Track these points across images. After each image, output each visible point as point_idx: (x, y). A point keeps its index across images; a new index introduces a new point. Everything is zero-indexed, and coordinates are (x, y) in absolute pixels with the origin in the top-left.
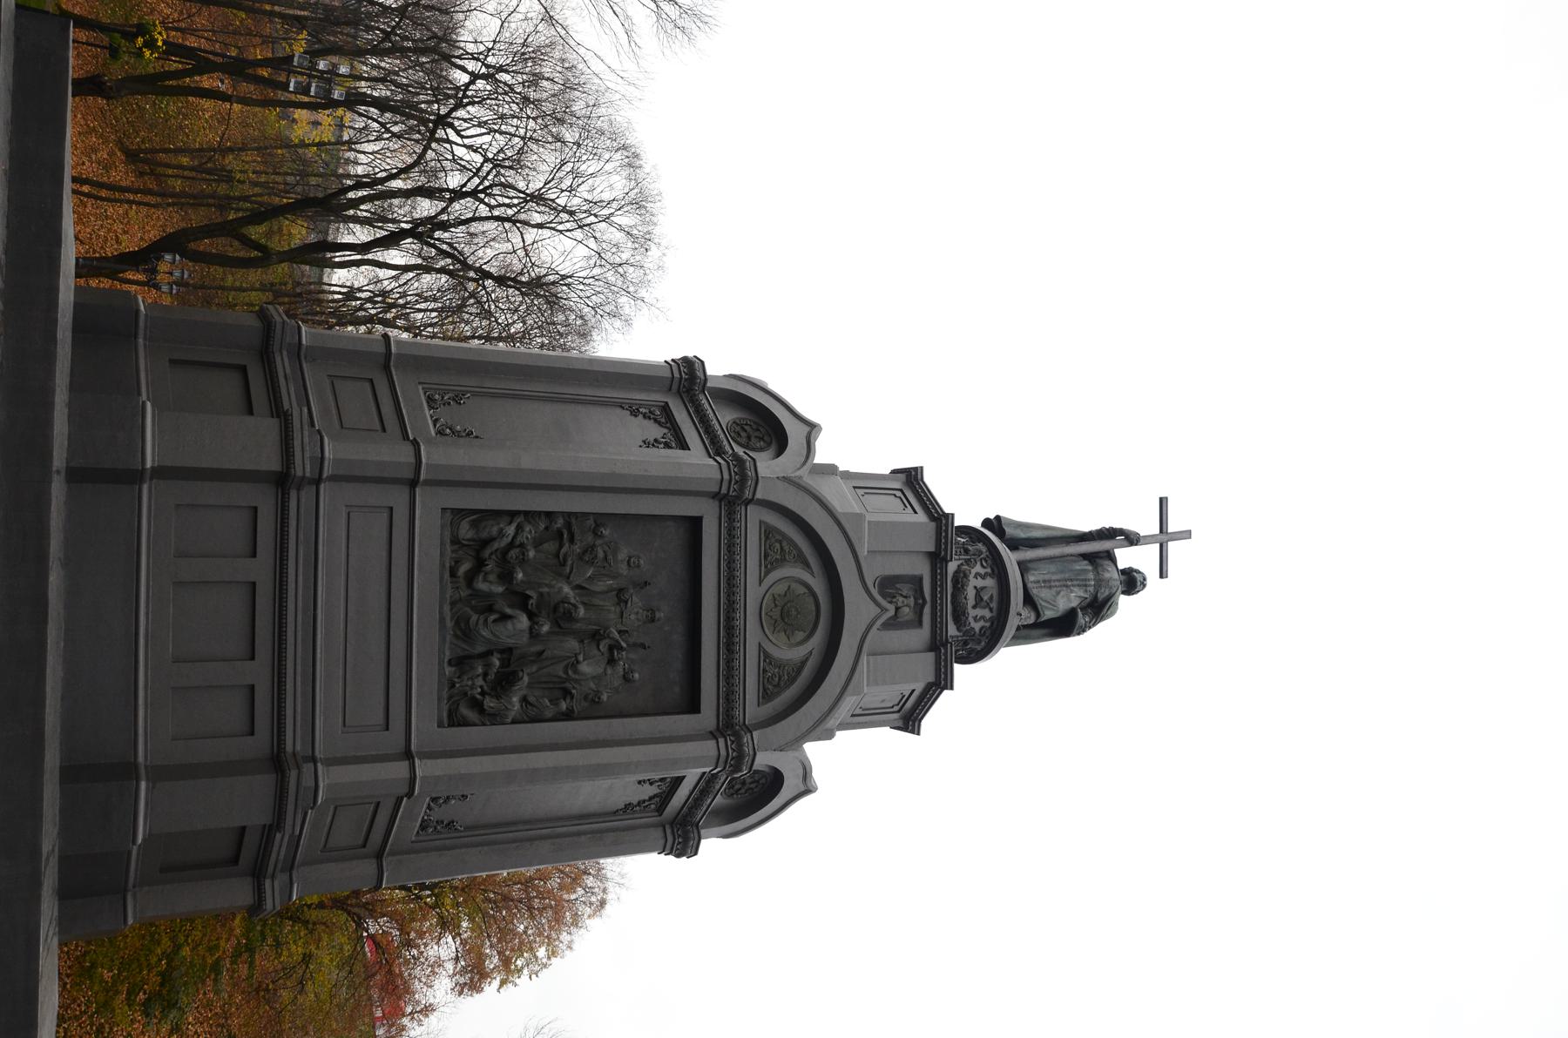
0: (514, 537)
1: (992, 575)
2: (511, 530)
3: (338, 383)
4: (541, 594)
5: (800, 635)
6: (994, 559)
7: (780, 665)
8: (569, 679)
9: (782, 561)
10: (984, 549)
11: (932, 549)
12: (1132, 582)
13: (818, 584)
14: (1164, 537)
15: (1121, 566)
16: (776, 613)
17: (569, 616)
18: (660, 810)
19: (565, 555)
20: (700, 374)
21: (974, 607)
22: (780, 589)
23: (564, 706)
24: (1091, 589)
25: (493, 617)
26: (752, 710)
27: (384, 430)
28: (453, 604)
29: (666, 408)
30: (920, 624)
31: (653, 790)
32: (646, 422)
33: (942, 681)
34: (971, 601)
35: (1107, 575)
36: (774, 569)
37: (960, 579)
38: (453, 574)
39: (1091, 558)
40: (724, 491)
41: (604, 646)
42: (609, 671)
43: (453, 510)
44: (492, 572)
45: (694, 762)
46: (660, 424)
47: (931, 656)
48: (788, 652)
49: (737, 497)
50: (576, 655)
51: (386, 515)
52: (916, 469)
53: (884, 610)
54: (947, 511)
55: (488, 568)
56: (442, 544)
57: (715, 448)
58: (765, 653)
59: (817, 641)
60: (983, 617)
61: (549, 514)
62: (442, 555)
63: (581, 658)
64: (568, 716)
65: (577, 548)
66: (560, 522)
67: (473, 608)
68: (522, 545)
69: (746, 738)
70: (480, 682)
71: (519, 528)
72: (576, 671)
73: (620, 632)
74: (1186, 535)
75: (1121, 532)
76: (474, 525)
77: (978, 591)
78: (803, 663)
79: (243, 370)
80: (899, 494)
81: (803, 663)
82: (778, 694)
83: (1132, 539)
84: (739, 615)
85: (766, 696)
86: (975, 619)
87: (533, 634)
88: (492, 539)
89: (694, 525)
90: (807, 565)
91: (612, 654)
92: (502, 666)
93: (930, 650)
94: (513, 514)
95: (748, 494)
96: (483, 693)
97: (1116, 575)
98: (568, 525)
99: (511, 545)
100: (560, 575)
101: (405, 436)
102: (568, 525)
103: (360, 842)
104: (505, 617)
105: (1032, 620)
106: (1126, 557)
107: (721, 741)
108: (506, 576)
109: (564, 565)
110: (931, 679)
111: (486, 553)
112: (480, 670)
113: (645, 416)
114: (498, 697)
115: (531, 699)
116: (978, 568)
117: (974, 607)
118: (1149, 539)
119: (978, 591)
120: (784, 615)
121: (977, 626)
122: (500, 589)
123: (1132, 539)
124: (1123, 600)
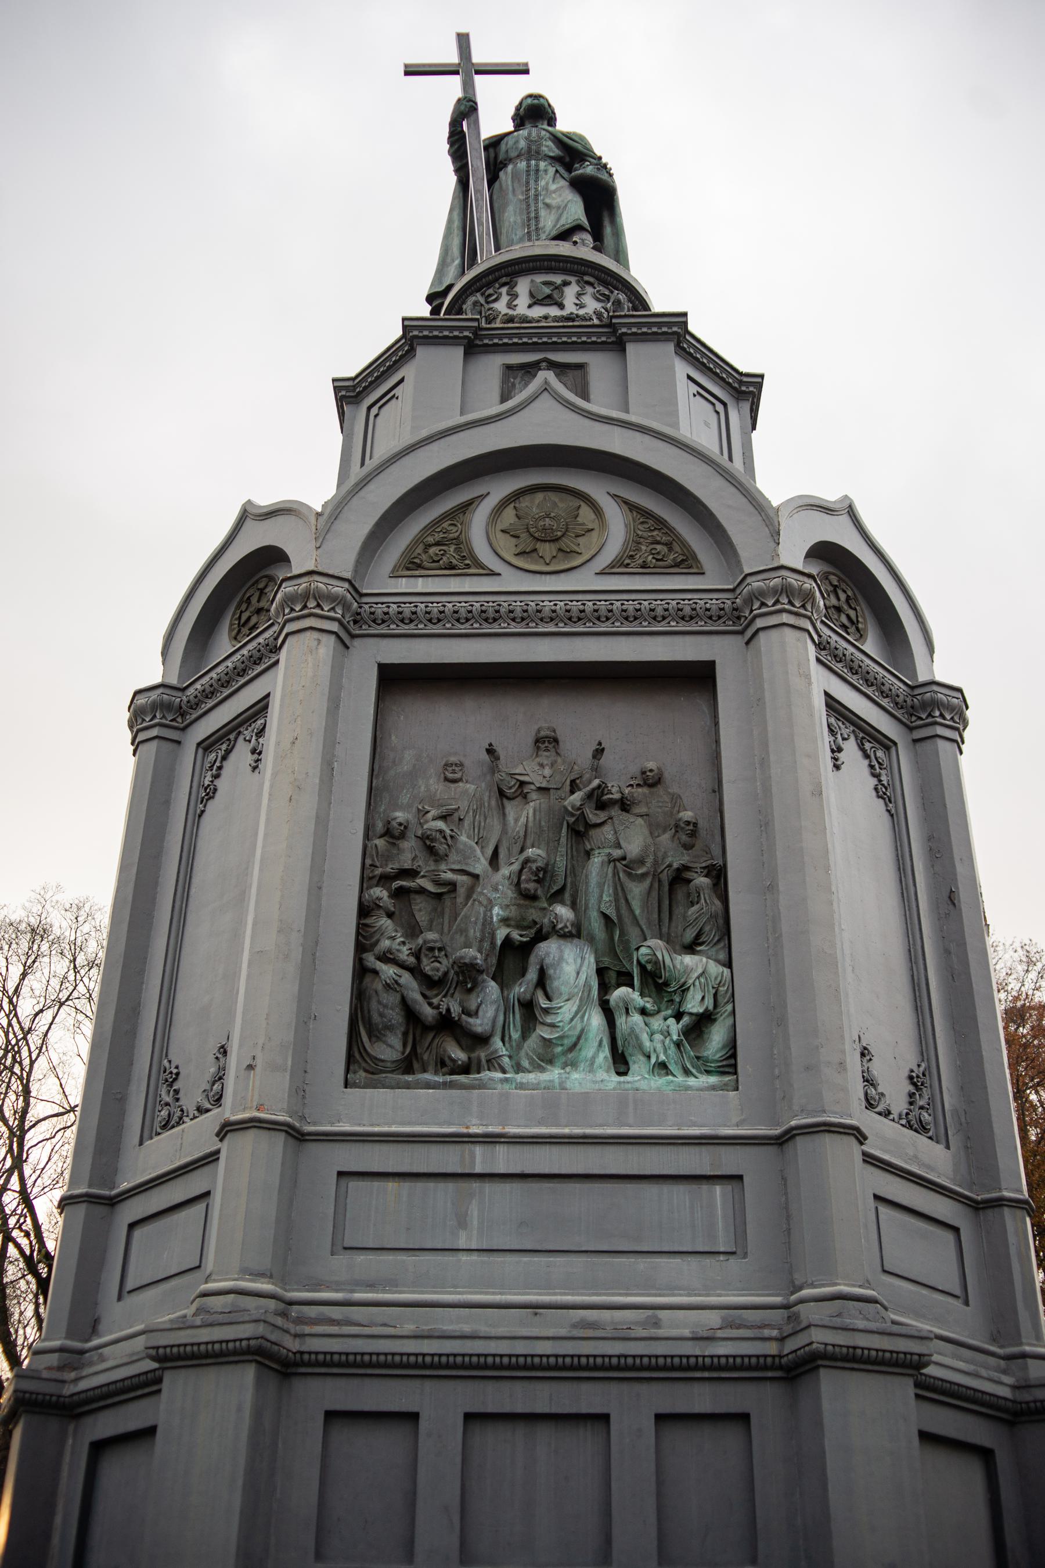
0: (402, 965)
1: (511, 285)
2: (388, 971)
3: (130, 1285)
4: (505, 921)
5: (586, 514)
6: (489, 285)
7: (634, 542)
8: (656, 876)
9: (461, 543)
10: (471, 300)
11: (460, 352)
12: (534, 112)
13: (499, 488)
14: (466, 68)
15: (510, 127)
16: (547, 550)
17: (543, 875)
18: (887, 744)
19: (437, 883)
20: (154, 695)
21: (561, 306)
22: (507, 546)
23: (702, 881)
24: (542, 165)
25: (544, 1003)
26: (712, 577)
27: (207, 1194)
28: (519, 1068)
29: (206, 745)
30: (580, 367)
31: (850, 747)
32: (224, 772)
33: (674, 330)
34: (554, 311)
35: (522, 144)
36: (471, 552)
38: (466, 1069)
39: (494, 170)
40: (334, 627)
41: (593, 816)
42: (637, 810)
43: (347, 1071)
44: (461, 1004)
45: (797, 675)
46: (228, 752)
47: (630, 348)
48: (617, 528)
49: (346, 607)
50: (612, 860)
51: (354, 1184)
52: (336, 389)
53: (546, 388)
54: (399, 333)
55: (456, 1009)
56: (408, 1086)
57: (265, 659)
58: (612, 565)
59: (598, 489)
60: (579, 295)
61: (365, 911)
62: (428, 1086)
63: (617, 853)
64: (718, 875)
65: (425, 865)
66: (380, 893)
67: (524, 1036)
68: (417, 955)
69: (756, 584)
70: (657, 1023)
71: (386, 958)
72: (641, 862)
73: (572, 792)
74: (463, 41)
75: (455, 125)
76: (375, 1034)
77: (536, 301)
78: (632, 507)
79: (99, 1448)
80: (374, 411)
81: (632, 507)
82: (684, 544)
83: (466, 110)
84: (547, 604)
85: (687, 564)
86: (581, 306)
87: (575, 933)
88: (404, 1000)
89: (394, 680)
90: (466, 507)
91: (613, 802)
92: (632, 986)
93: (624, 350)
94: (362, 972)
95: (339, 589)
96: (678, 1016)
97: (523, 133)
98: (385, 879)
99: (415, 971)
100: (470, 891)
101: (213, 1157)
102: (385, 879)
103: (949, 1236)
104: (542, 982)
105: (589, 238)
106: (495, 118)
107: (760, 623)
108: (468, 977)
109: (453, 886)
110: (670, 347)
111: (428, 1012)
112: (637, 1018)
113: (217, 776)
114: (684, 990)
115: (689, 936)
116: (501, 306)
117: (561, 306)
118: (468, 86)
119: (536, 301)
120: (547, 541)
121: (591, 305)
122: (492, 988)
123: (466, 110)
124: (563, 125)
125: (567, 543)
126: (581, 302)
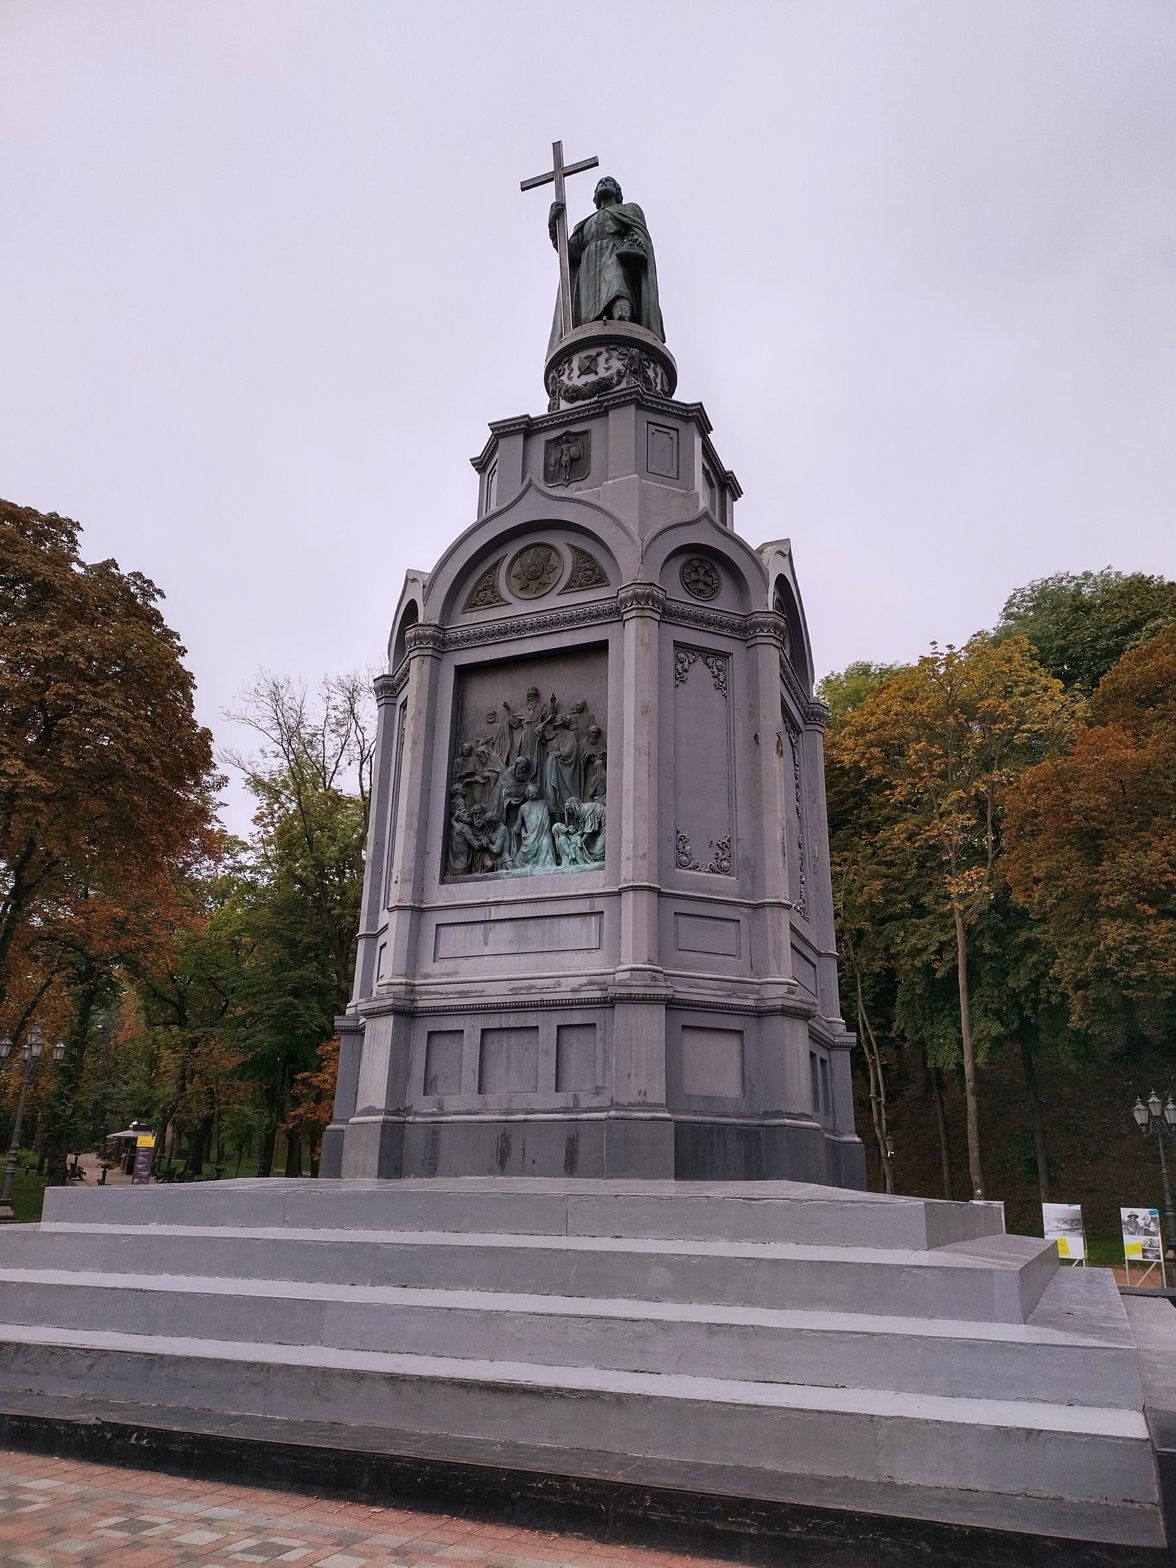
9: (493, 588)
16: (533, 584)
21: (596, 373)
34: (591, 378)
37: (573, 395)
58: (565, 589)
85: (600, 580)
86: (607, 369)
90: (496, 566)
117: (596, 373)
120: (534, 580)
125: (544, 579)
126: (610, 365)
